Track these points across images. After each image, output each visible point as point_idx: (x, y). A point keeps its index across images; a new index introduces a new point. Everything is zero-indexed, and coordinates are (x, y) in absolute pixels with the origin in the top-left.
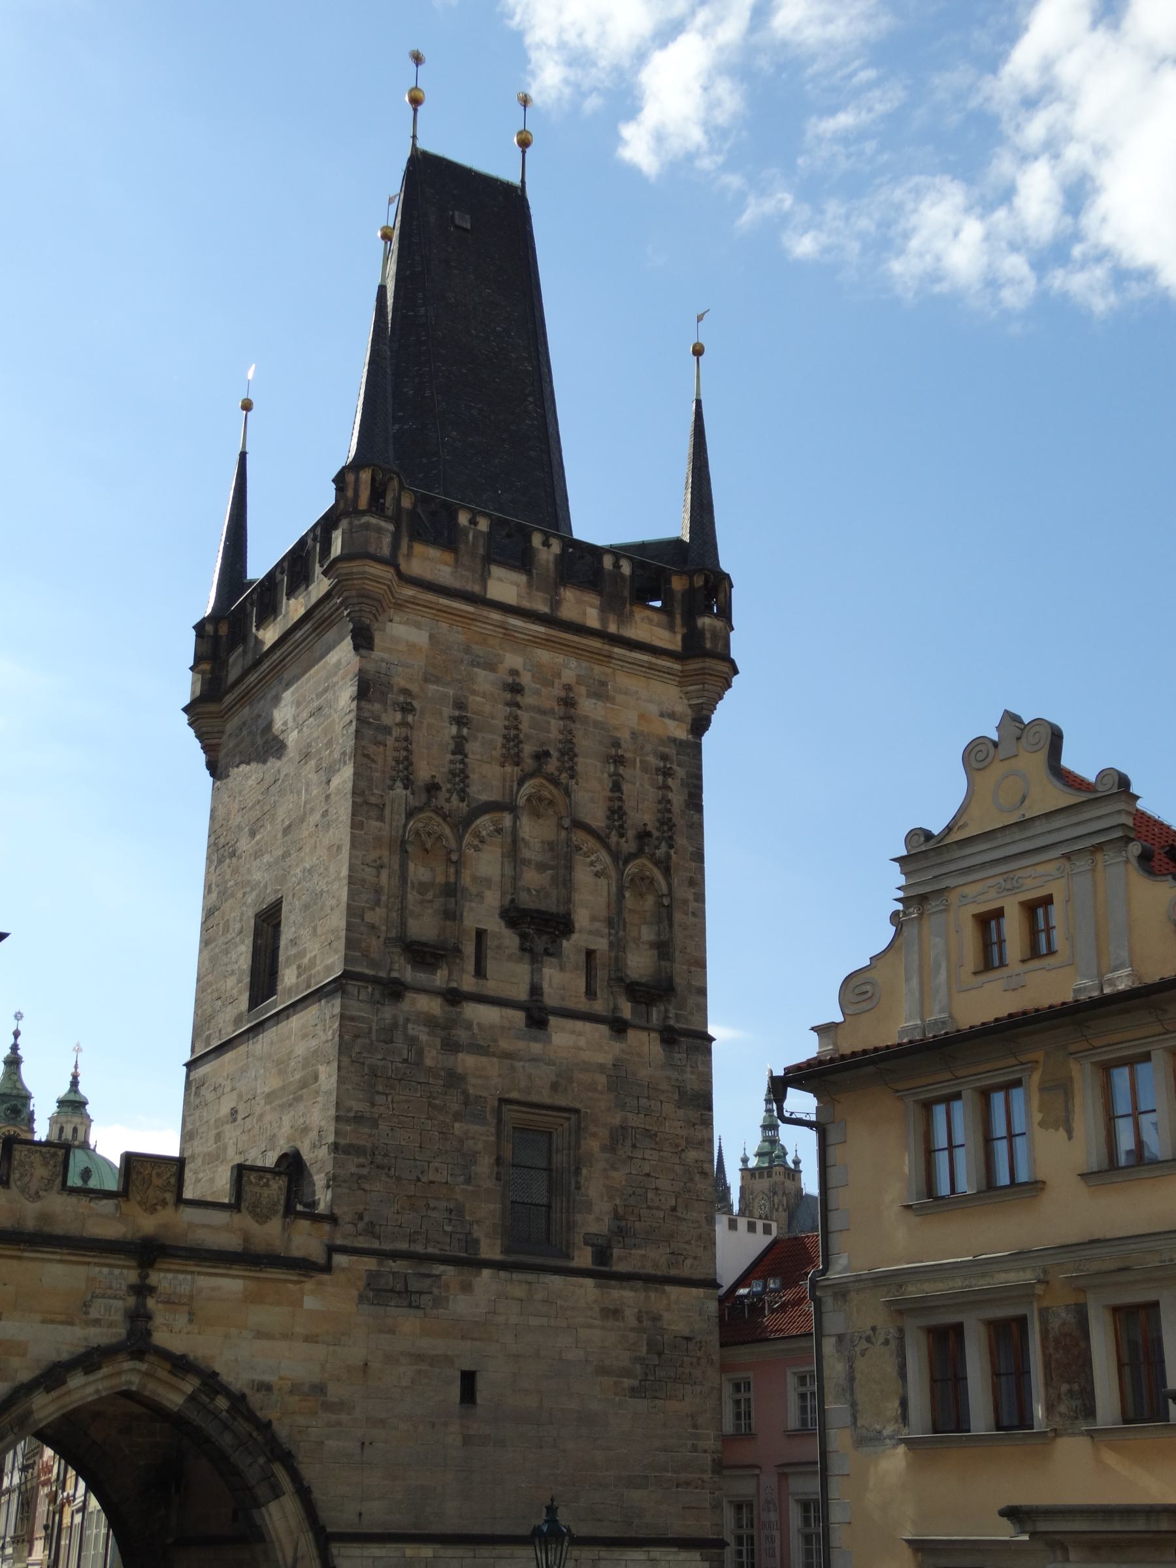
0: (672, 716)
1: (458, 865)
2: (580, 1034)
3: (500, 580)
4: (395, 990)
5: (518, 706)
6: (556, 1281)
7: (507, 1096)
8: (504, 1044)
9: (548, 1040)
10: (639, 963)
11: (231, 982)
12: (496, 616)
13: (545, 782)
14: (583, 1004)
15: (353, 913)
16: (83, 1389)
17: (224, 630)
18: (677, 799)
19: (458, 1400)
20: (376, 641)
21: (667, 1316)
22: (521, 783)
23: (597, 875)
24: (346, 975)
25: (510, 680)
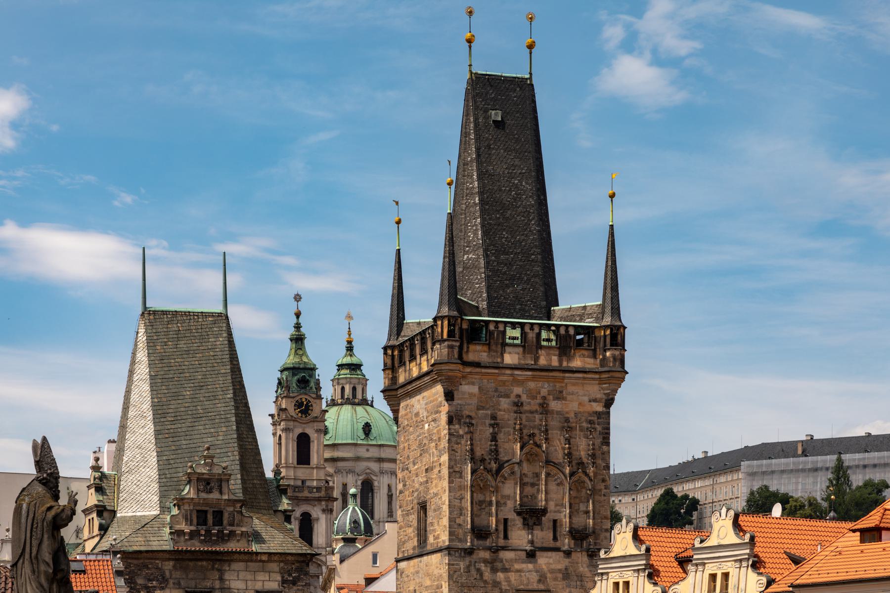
0: (595, 400)
1: (497, 490)
11: (410, 530)
12: (508, 372)
15: (451, 520)
18: (598, 441)
25: (516, 400)
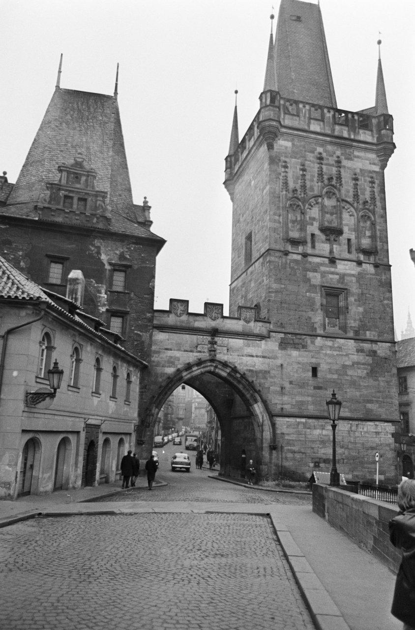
0: (374, 164)
1: (303, 213)
2: (347, 265)
3: (314, 124)
4: (286, 253)
5: (322, 164)
6: (342, 341)
7: (323, 285)
8: (323, 269)
9: (336, 268)
10: (366, 242)
12: (313, 136)
13: (332, 188)
14: (348, 256)
16: (196, 371)
17: (233, 159)
19: (311, 376)
20: (275, 146)
21: (378, 352)
22: (323, 188)
23: (351, 216)
24: (268, 250)
25: (319, 156)
